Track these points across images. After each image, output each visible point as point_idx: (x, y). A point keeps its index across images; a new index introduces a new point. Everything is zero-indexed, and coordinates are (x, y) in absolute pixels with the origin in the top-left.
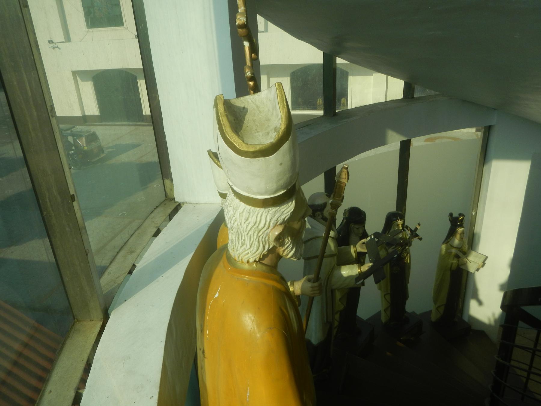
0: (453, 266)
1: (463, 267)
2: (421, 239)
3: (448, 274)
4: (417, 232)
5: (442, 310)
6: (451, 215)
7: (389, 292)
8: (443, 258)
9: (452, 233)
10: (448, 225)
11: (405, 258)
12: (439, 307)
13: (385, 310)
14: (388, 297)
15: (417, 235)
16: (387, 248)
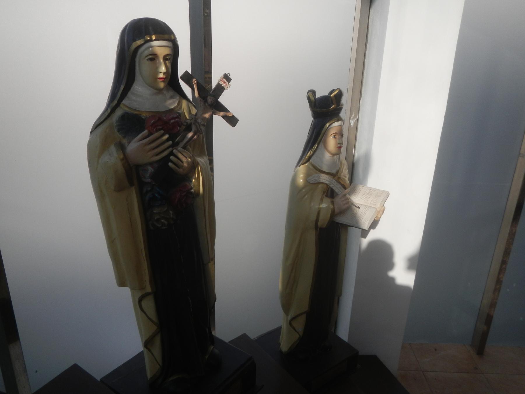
0: (321, 217)
1: (342, 220)
2: (232, 121)
3: (312, 237)
4: (222, 99)
5: (300, 325)
6: (313, 92)
7: (149, 289)
8: (298, 196)
9: (316, 137)
10: (306, 118)
11: (187, 177)
12: (294, 318)
13: (147, 344)
14: (149, 304)
15: (219, 108)
16: (125, 141)
